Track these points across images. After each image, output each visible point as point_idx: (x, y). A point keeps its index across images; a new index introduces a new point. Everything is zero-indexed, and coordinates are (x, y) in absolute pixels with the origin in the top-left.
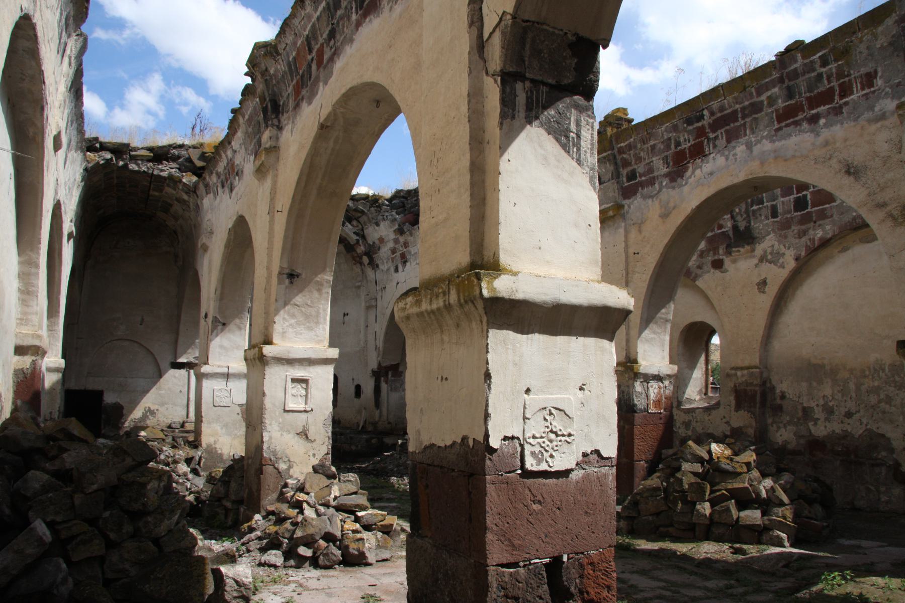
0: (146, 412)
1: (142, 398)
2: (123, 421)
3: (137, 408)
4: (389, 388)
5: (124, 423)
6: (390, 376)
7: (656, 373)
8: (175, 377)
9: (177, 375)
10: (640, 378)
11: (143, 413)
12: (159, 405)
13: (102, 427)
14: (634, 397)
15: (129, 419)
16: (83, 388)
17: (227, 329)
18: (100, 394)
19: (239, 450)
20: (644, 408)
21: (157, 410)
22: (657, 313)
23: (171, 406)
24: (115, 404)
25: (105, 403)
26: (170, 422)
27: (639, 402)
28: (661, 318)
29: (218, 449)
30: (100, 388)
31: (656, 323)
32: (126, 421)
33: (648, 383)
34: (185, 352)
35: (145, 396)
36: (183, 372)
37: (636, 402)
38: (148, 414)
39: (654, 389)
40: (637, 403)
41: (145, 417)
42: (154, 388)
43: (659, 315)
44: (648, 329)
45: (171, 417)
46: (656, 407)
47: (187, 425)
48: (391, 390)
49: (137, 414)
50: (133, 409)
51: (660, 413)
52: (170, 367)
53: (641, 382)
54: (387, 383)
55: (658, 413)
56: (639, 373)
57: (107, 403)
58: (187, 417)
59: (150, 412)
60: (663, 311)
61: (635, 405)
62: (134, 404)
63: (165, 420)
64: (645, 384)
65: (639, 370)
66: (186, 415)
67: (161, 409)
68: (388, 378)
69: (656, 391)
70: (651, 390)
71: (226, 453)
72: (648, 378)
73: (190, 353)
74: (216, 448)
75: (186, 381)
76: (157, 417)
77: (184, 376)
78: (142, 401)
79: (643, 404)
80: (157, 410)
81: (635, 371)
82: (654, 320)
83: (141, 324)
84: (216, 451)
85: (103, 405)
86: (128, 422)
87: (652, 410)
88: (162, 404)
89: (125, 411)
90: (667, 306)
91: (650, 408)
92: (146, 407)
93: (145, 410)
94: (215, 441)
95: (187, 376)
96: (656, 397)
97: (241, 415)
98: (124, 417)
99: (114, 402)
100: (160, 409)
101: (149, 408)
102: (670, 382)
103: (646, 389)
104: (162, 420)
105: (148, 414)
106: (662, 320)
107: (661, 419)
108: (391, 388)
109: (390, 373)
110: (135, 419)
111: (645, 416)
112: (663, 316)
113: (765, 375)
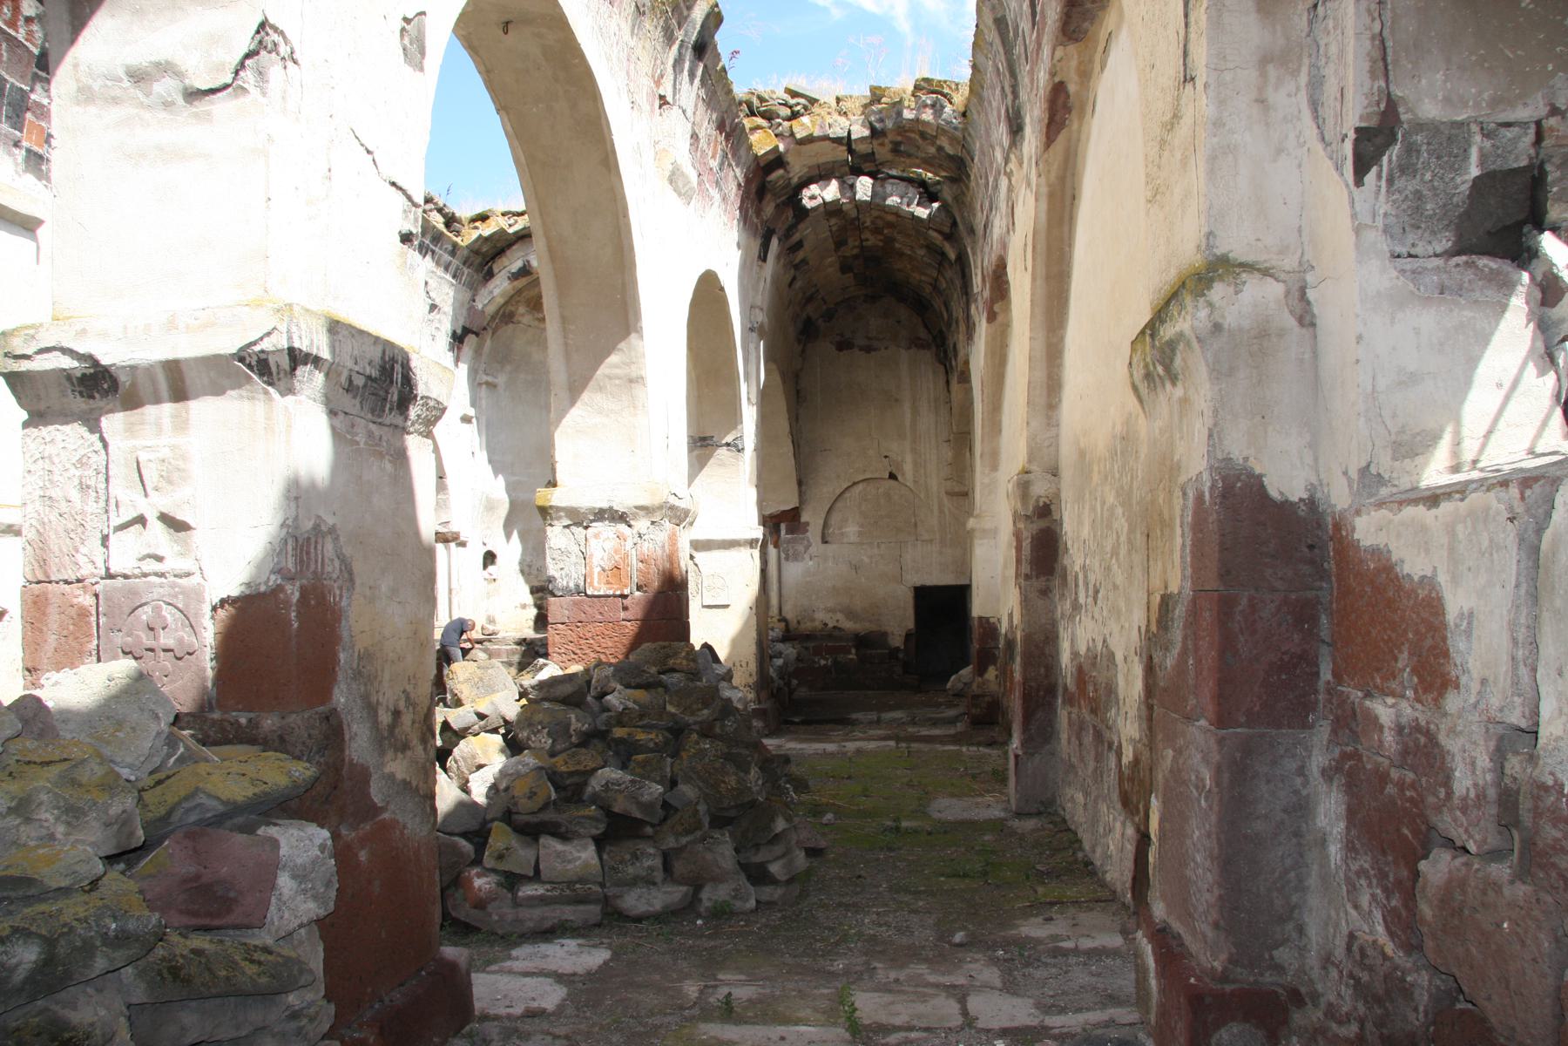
4: (783, 555)
6: (783, 532)
7: (605, 505)
10: (559, 518)
14: (548, 560)
20: (577, 586)
22: (595, 369)
27: (563, 569)
28: (610, 378)
31: (601, 389)
33: (586, 528)
37: (552, 570)
39: (603, 541)
40: (557, 575)
43: (603, 370)
44: (579, 404)
46: (608, 583)
48: (787, 559)
51: (624, 597)
53: (565, 527)
54: (776, 546)
55: (615, 596)
56: (551, 507)
60: (613, 359)
61: (551, 580)
64: (579, 531)
65: (549, 500)
68: (779, 536)
69: (609, 545)
70: (593, 542)
72: (579, 519)
79: (574, 575)
81: (540, 503)
82: (592, 383)
87: (598, 587)
90: (622, 345)
91: (591, 584)
96: (609, 559)
102: (653, 523)
103: (583, 543)
106: (617, 382)
107: (625, 609)
108: (787, 555)
109: (783, 526)
111: (575, 603)
112: (617, 371)
113: (1040, 489)
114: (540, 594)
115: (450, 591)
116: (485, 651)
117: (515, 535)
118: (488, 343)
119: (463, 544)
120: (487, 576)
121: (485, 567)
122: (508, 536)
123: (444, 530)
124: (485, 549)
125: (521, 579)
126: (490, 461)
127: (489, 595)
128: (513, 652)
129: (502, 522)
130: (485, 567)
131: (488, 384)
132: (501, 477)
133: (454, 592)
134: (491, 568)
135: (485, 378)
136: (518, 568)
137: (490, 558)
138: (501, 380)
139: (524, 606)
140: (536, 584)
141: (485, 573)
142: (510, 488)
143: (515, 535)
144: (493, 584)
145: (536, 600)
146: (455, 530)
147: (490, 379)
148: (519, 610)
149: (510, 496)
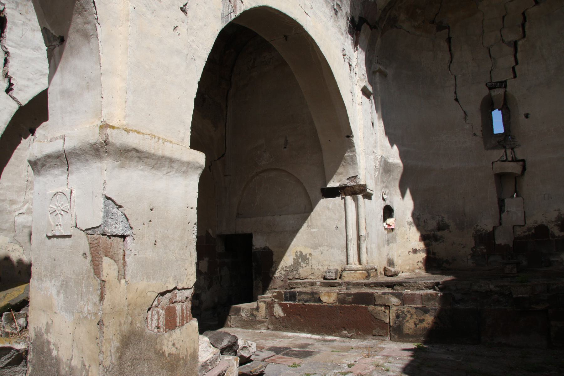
0: (298, 258)
1: (292, 240)
2: (273, 269)
3: (287, 254)
5: (274, 273)
8: (328, 209)
9: (330, 206)
11: (294, 259)
12: (312, 248)
13: (254, 277)
15: (280, 267)
16: (233, 233)
17: (67, 45)
18: (249, 237)
19: (56, 354)
21: (310, 254)
23: (326, 248)
24: (264, 249)
25: (254, 248)
26: (325, 269)
29: (52, 347)
30: (248, 231)
32: (276, 270)
34: (333, 172)
35: (294, 236)
36: (337, 201)
38: (300, 260)
41: (296, 265)
42: (305, 225)
45: (327, 263)
47: (344, 274)
49: (288, 260)
50: (283, 254)
52: (321, 196)
57: (257, 249)
58: (347, 264)
59: (302, 258)
62: (284, 247)
63: (320, 267)
66: (345, 260)
67: (315, 253)
71: (64, 360)
73: (342, 173)
74: (49, 342)
75: (344, 213)
76: (310, 264)
77: (340, 206)
78: (293, 243)
80: (310, 254)
83: (285, 148)
84: (50, 351)
85: (253, 251)
86: (278, 270)
88: (315, 247)
89: (274, 258)
92: (297, 252)
93: (296, 255)
94: (47, 324)
95: (343, 206)
97: (89, 258)
98: (274, 265)
99: (263, 247)
100: (313, 253)
101: (301, 252)
104: (316, 268)
105: (300, 260)
110: (286, 267)
114: (427, 241)
115: (359, 237)
116: (398, 296)
117: (408, 193)
118: (379, 40)
119: (368, 196)
120: (386, 227)
121: (385, 220)
122: (403, 195)
123: (352, 184)
124: (383, 205)
125: (414, 229)
126: (387, 133)
127: (388, 242)
128: (429, 298)
129: (397, 184)
130: (385, 220)
131: (380, 71)
132: (395, 147)
133: (362, 239)
134: (389, 221)
135: (378, 66)
136: (411, 219)
137: (388, 212)
138: (390, 72)
139: (415, 251)
140: (424, 233)
141: (385, 224)
142: (403, 156)
143: (408, 193)
144: (391, 234)
145: (426, 245)
146: (362, 183)
147: (382, 68)
148: (411, 254)
149: (402, 161)
